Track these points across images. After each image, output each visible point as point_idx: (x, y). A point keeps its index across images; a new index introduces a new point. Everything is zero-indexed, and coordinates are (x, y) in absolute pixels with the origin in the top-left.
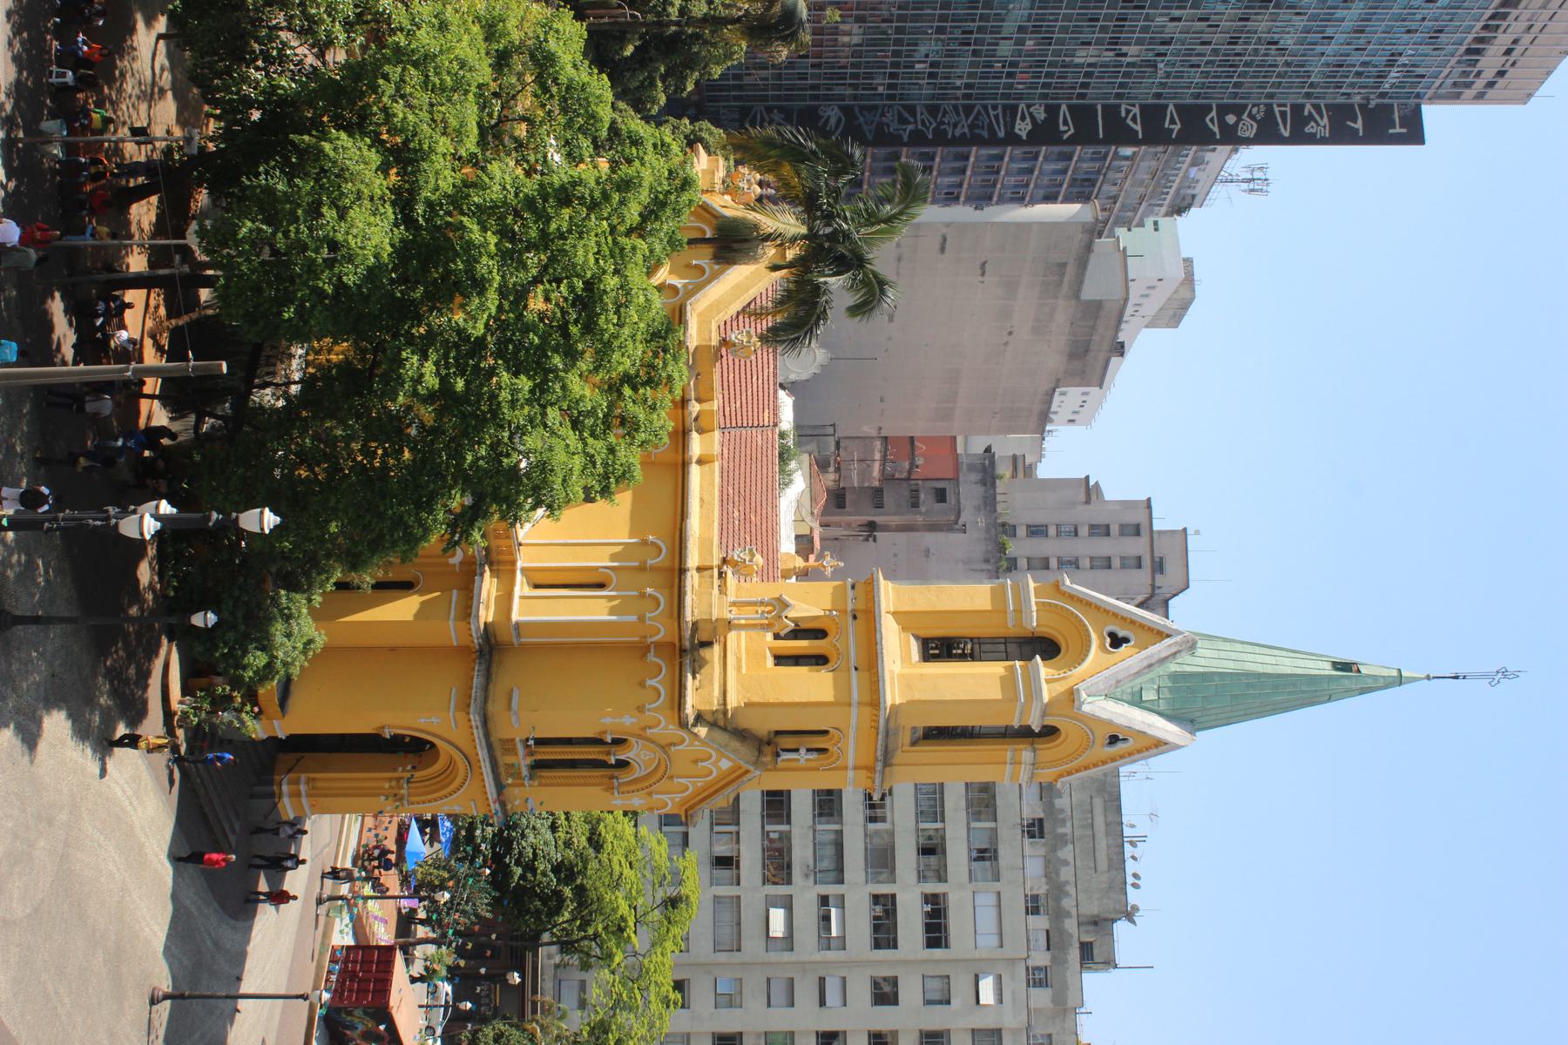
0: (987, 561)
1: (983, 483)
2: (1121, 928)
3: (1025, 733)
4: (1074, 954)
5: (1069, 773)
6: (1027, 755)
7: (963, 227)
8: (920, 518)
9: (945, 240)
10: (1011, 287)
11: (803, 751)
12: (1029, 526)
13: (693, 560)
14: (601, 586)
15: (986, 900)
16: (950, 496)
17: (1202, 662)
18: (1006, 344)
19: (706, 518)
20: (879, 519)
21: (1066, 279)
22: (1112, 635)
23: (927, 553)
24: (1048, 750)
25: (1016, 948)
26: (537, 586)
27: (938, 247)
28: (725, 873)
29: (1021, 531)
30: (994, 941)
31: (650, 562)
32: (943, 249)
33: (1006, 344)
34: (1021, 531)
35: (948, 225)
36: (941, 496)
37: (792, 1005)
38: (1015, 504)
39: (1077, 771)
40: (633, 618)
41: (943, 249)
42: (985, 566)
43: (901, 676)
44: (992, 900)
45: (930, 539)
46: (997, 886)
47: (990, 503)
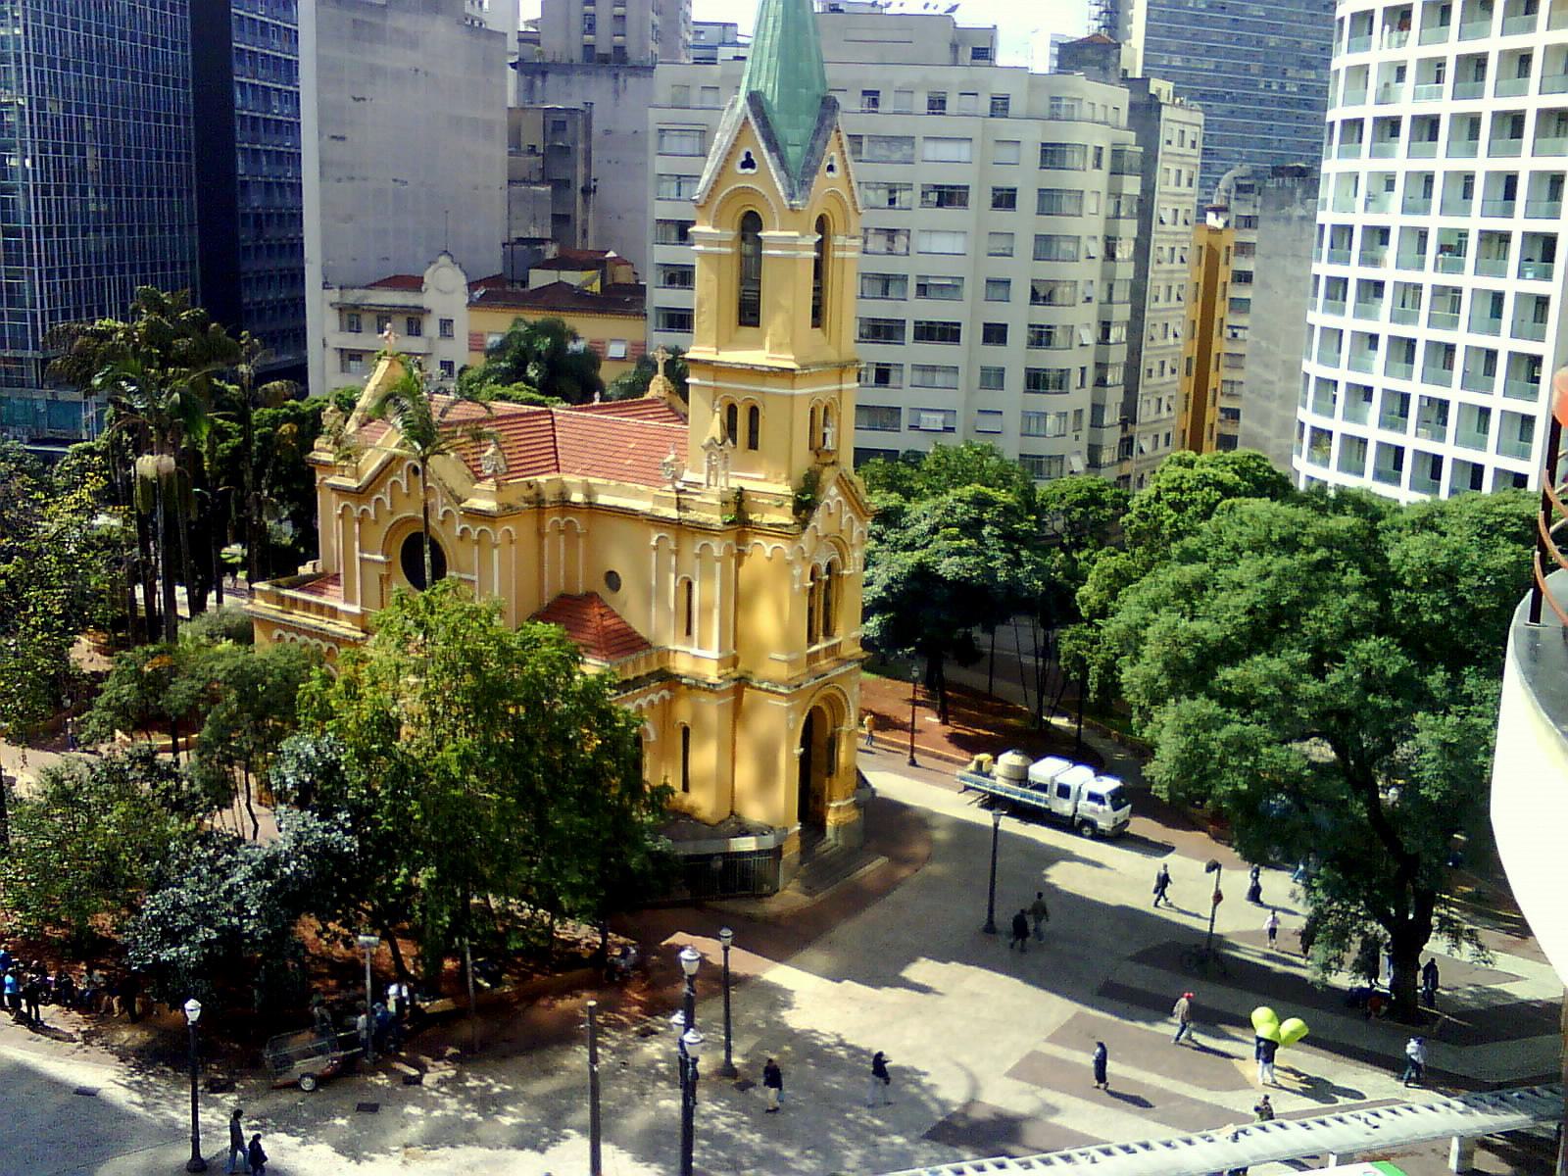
0: (616, 76)
1: (544, 74)
2: (962, 19)
3: (820, 246)
4: (981, 72)
5: (855, 203)
6: (839, 240)
7: (322, 121)
8: (581, 146)
9: (334, 137)
10: (374, 72)
11: (827, 430)
12: (585, 33)
13: (673, 514)
14: (690, 585)
15: (932, 150)
16: (563, 116)
17: (770, 85)
18: (426, 74)
19: (638, 495)
20: (580, 184)
21: (367, 19)
22: (744, 165)
23: (608, 132)
24: (836, 224)
25: (971, 128)
26: (689, 632)
27: (340, 143)
28: (894, 376)
29: (589, 38)
30: (966, 146)
31: (673, 547)
32: (343, 138)
33: (426, 74)
34: (589, 38)
35: (320, 134)
36: (559, 127)
37: (1008, 282)
38: (560, 45)
39: (853, 196)
40: (718, 565)
41: (343, 138)
42: (621, 79)
43: (771, 351)
44: (931, 145)
45: (597, 128)
46: (919, 141)
47: (566, 68)
